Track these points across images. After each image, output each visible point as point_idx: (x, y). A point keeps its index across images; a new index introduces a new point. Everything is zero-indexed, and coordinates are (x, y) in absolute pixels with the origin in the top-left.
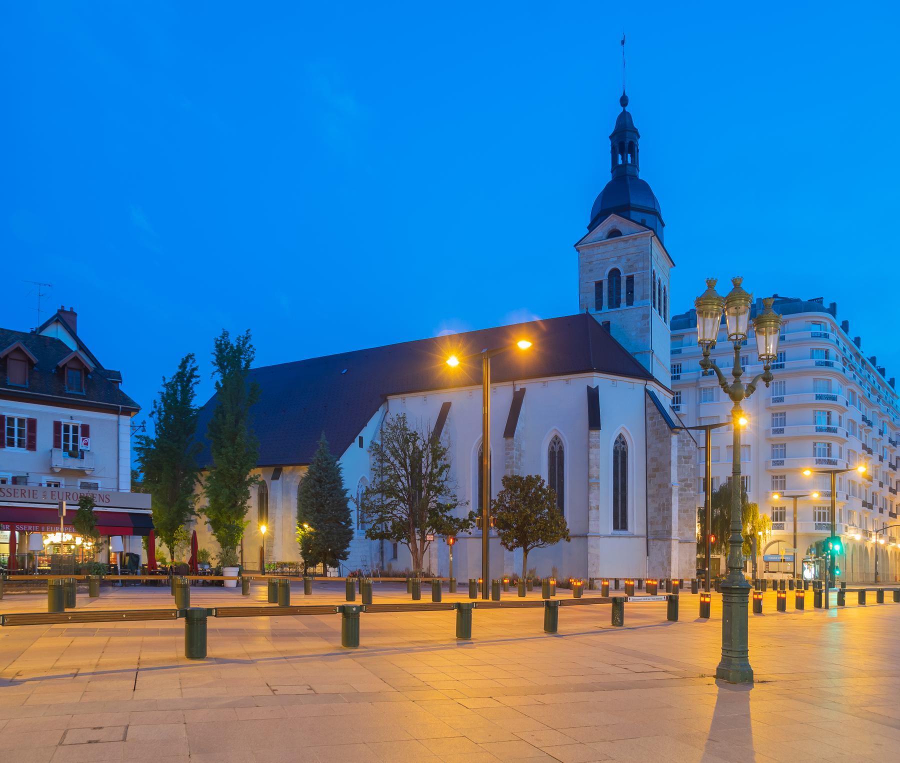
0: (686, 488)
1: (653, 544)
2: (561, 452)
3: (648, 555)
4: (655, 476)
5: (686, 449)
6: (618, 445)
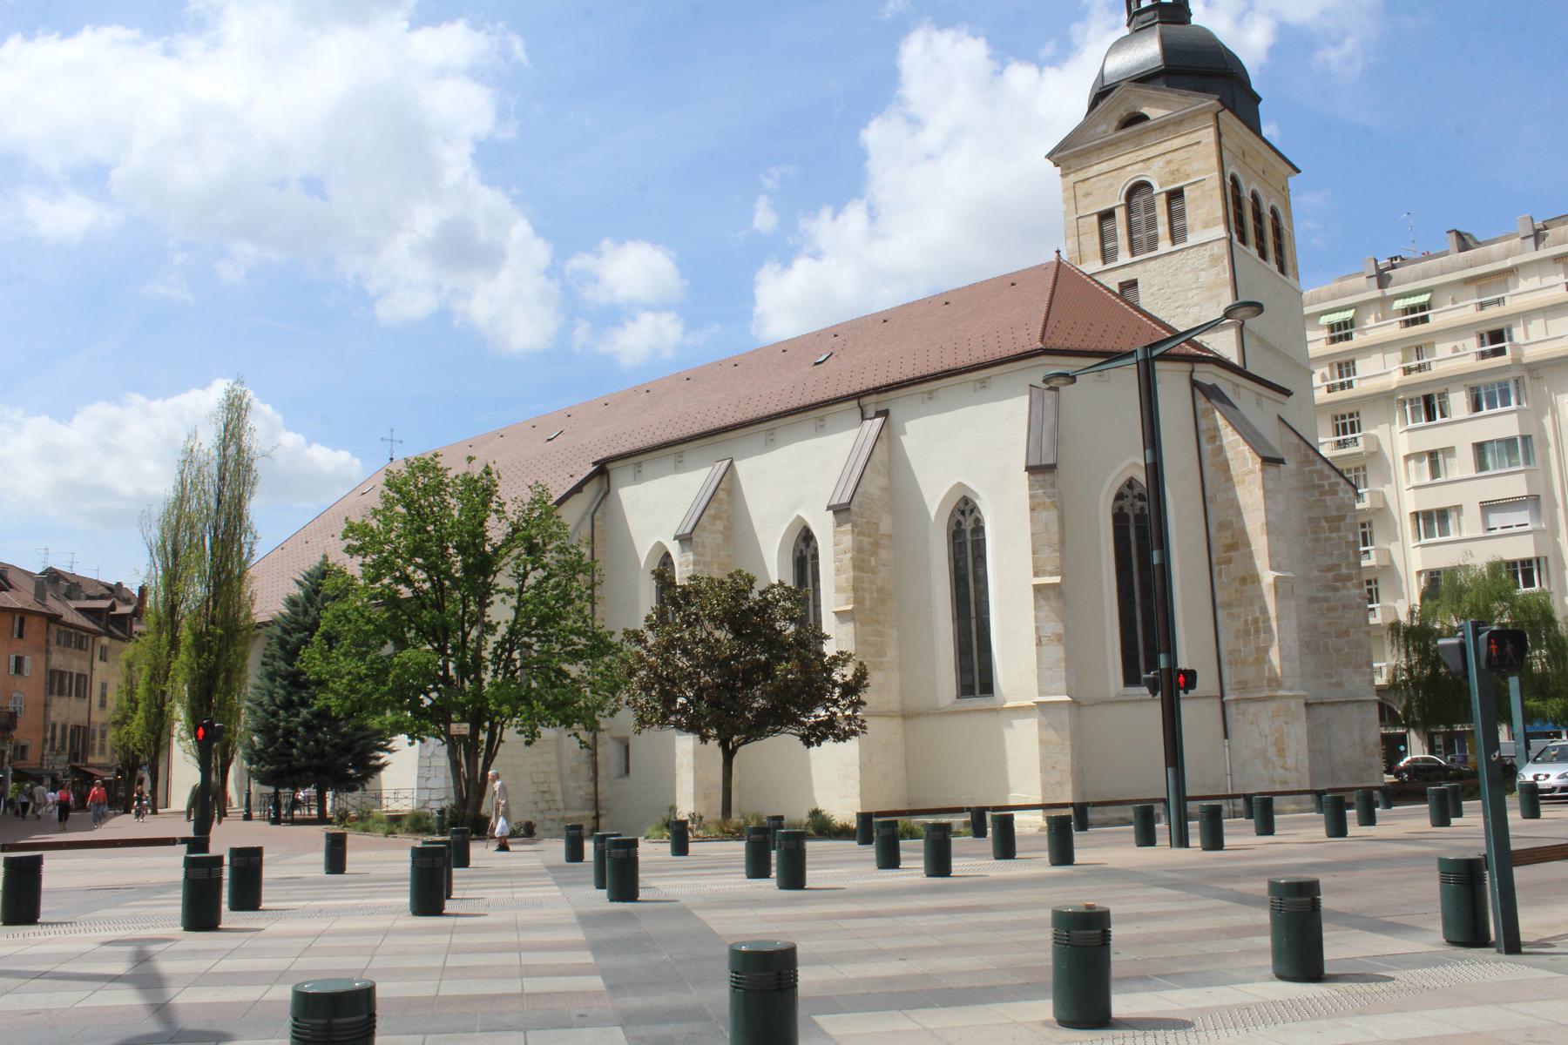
0: (1338, 584)
1: (1237, 709)
2: (979, 529)
3: (1226, 737)
4: (1229, 561)
5: (1329, 500)
6: (1126, 503)
